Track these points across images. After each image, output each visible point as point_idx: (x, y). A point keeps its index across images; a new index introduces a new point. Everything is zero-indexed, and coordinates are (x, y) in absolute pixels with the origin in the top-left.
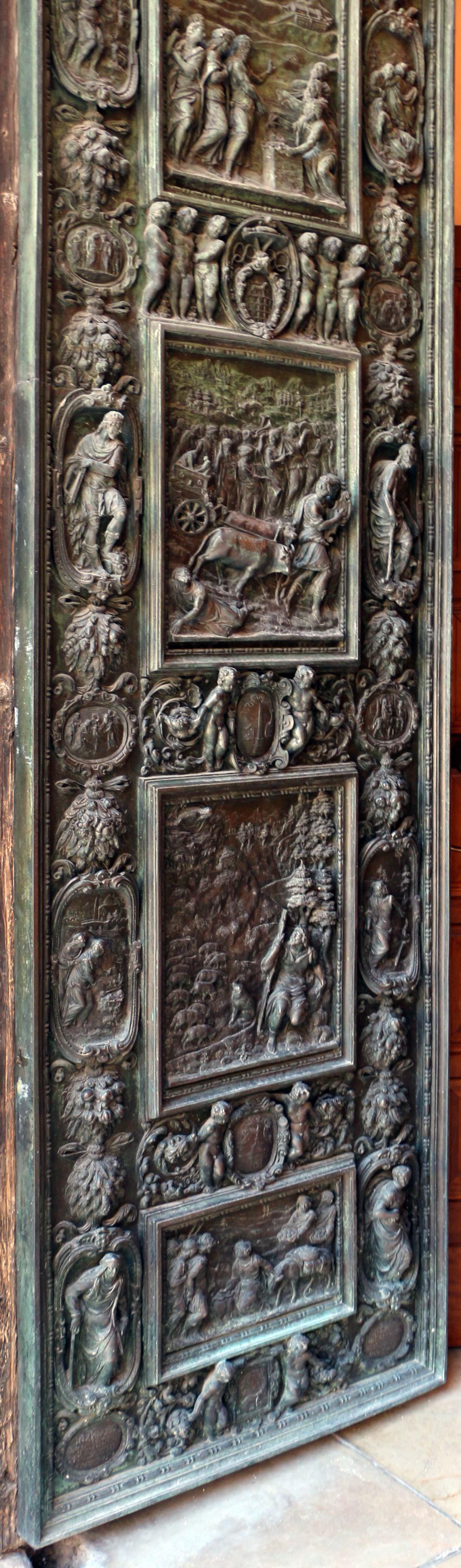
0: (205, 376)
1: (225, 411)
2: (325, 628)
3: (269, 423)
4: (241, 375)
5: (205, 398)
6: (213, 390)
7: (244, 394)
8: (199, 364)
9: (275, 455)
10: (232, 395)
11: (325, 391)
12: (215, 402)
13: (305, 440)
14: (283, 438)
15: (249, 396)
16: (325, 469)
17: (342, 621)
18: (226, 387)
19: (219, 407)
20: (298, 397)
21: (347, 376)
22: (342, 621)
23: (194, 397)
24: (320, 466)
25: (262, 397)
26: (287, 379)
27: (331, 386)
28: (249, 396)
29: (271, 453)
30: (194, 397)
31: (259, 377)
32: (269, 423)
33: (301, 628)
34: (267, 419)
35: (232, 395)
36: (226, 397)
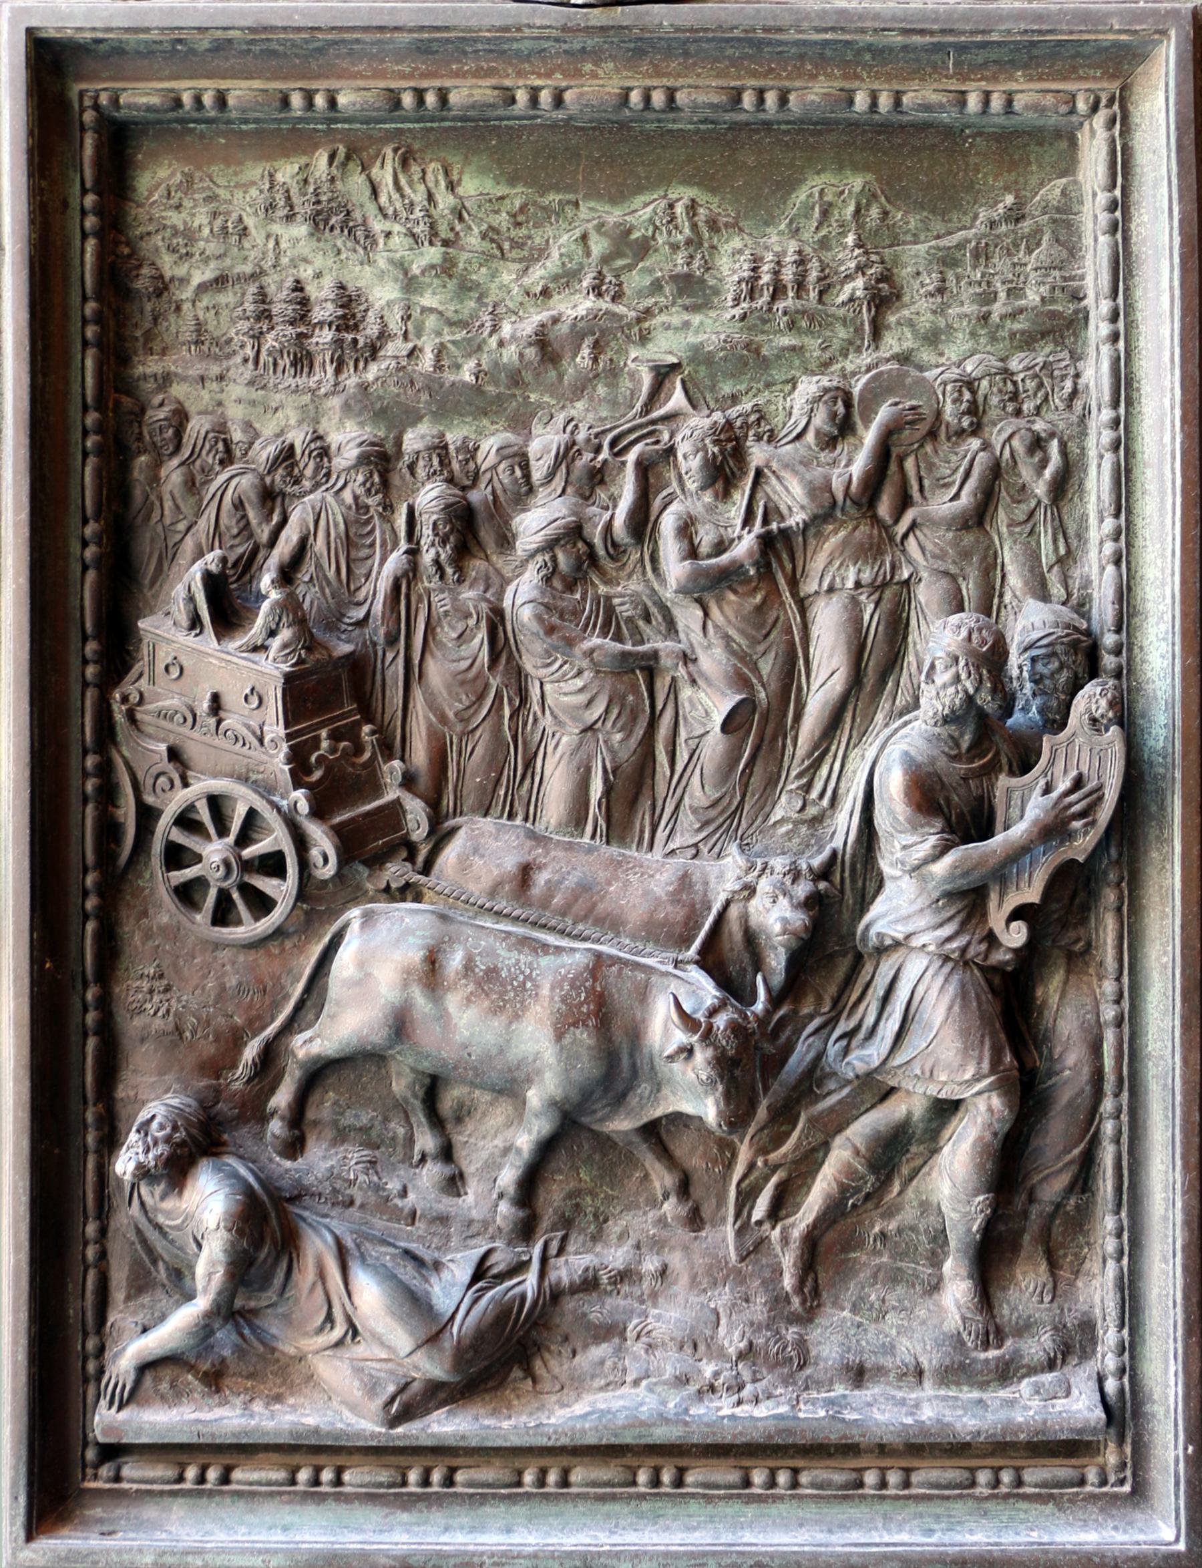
0: (319, 222)
1: (427, 362)
2: (1006, 1373)
3: (677, 399)
4: (518, 196)
5: (318, 314)
6: (360, 276)
7: (537, 275)
8: (287, 172)
9: (706, 537)
10: (466, 287)
11: (1016, 215)
12: (371, 329)
13: (884, 454)
14: (757, 454)
15: (567, 278)
16: (1015, 581)
17: (1110, 1336)
18: (433, 254)
19: (395, 348)
20: (847, 255)
21: (1123, 121)
22: (1110, 1336)
23: (264, 315)
24: (990, 568)
25: (636, 280)
26: (789, 185)
27: (1053, 191)
28: (567, 278)
29: (686, 530)
30: (264, 315)
31: (617, 197)
32: (677, 399)
33: (858, 1375)
34: (663, 375)
35: (466, 287)
36: (428, 300)
